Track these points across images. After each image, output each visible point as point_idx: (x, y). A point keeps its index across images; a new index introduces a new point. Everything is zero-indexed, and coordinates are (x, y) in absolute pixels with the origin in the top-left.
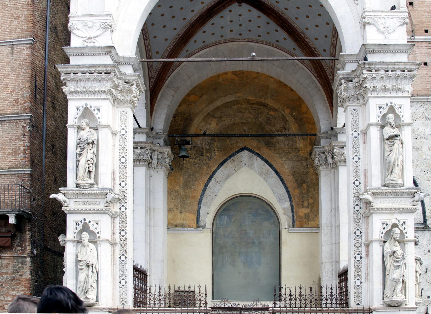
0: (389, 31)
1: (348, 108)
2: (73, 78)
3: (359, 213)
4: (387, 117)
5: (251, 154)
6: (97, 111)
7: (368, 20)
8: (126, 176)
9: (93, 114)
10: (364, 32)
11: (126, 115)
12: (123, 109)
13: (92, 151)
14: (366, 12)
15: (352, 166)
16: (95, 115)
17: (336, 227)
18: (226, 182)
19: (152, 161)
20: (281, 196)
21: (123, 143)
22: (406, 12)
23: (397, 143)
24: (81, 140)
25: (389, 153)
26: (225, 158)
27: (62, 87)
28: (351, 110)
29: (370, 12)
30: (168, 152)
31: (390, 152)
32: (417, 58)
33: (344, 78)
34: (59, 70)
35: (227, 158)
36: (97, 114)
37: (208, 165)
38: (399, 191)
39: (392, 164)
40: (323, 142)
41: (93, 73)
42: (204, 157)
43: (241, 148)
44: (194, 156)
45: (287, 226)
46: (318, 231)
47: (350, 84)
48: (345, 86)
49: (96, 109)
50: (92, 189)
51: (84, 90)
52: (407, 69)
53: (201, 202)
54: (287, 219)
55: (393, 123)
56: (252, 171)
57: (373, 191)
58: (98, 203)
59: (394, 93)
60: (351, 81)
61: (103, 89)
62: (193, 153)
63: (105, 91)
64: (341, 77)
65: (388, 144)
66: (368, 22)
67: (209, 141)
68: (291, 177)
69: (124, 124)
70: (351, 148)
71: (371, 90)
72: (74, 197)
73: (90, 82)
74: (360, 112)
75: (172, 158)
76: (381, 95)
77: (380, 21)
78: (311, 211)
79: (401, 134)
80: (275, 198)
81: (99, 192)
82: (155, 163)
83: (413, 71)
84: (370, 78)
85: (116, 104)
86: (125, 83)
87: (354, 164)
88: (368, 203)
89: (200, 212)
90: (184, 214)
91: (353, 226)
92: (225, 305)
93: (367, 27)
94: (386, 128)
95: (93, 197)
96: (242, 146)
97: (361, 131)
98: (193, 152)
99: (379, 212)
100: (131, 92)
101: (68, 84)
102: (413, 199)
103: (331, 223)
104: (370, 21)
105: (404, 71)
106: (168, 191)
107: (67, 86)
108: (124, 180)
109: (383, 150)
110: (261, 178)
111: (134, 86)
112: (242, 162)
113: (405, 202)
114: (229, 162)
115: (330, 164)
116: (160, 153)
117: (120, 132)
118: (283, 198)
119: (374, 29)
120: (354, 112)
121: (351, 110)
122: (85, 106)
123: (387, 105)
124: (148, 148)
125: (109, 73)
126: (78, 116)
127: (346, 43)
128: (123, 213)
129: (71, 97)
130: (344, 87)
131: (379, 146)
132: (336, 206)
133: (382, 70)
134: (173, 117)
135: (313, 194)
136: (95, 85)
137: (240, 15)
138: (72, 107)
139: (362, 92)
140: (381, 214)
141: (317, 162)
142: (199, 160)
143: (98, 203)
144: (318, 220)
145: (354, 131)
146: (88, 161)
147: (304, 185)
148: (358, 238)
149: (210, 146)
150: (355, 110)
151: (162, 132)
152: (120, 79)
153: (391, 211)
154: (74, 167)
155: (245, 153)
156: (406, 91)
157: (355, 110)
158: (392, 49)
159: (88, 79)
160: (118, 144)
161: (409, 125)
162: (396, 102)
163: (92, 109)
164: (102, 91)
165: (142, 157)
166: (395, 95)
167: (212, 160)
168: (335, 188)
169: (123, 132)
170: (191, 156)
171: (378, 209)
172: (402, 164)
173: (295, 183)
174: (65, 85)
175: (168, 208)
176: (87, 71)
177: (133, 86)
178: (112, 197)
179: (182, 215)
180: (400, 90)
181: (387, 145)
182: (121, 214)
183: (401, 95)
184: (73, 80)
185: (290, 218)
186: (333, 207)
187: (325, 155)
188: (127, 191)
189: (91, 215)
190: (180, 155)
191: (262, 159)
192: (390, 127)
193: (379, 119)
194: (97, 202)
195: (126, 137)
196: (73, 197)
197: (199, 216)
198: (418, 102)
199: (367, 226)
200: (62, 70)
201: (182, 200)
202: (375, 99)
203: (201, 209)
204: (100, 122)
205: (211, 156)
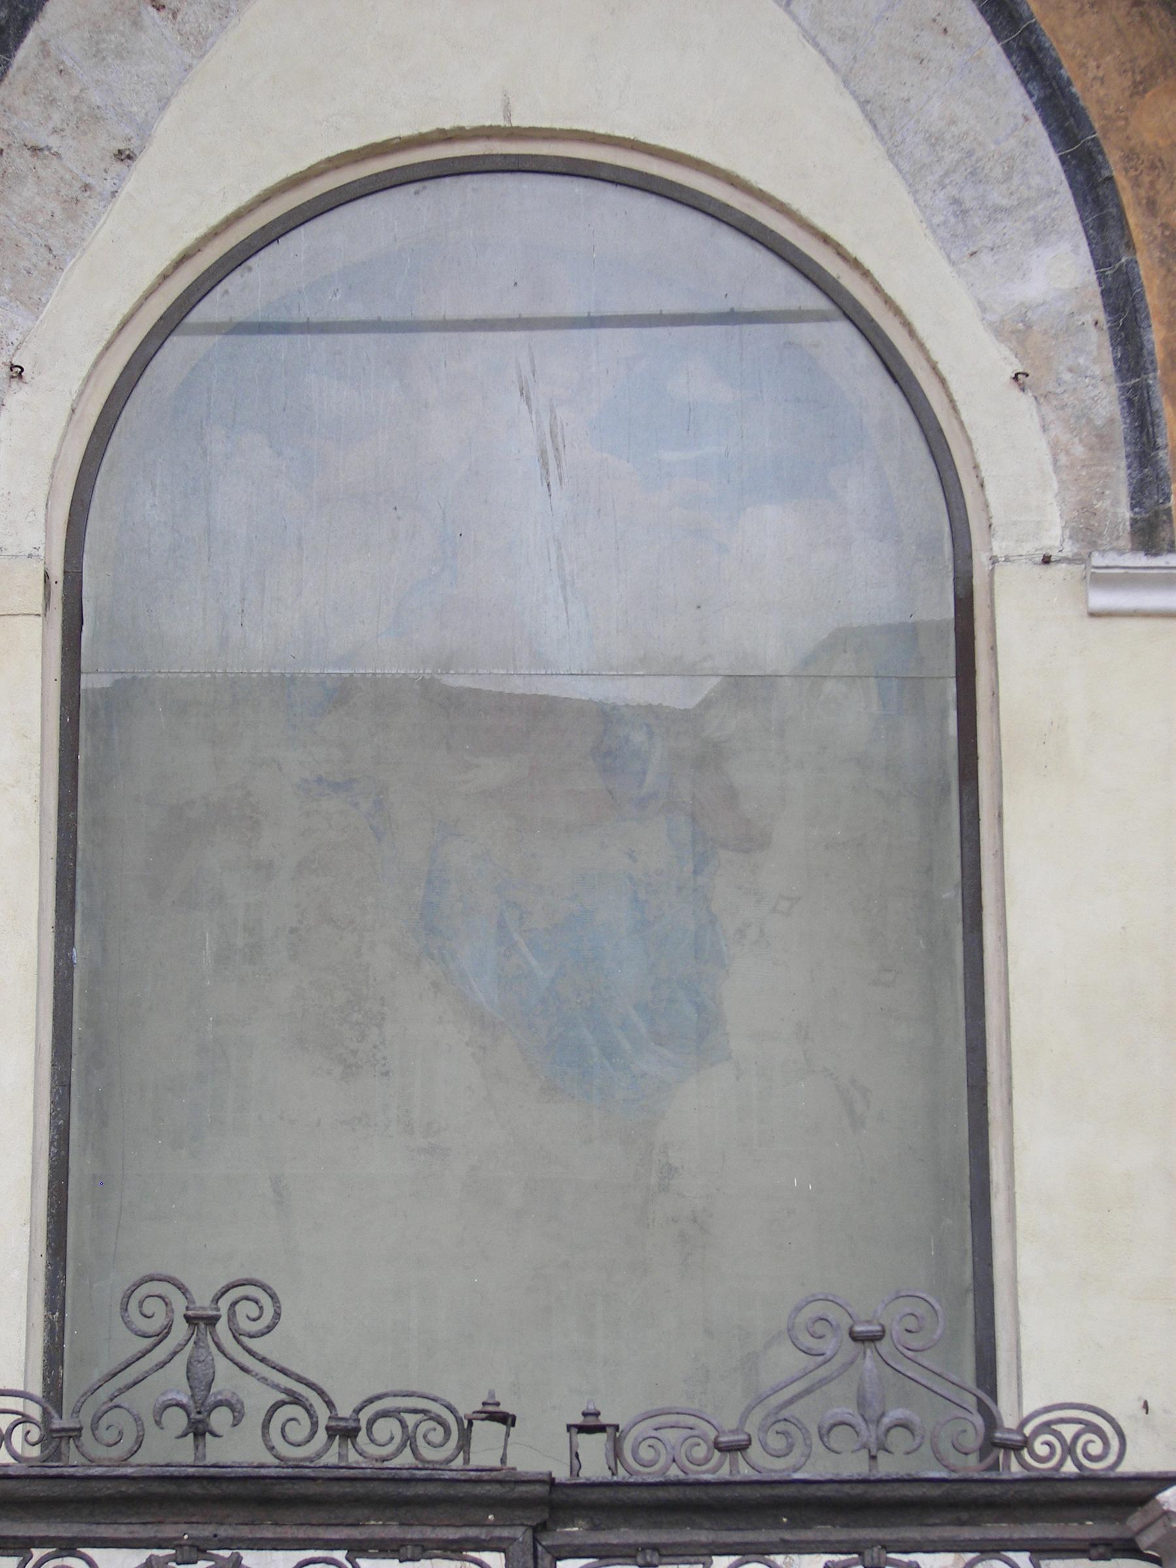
20: (975, 175)
92: (199, 1430)
118: (997, 197)
185: (1102, 440)
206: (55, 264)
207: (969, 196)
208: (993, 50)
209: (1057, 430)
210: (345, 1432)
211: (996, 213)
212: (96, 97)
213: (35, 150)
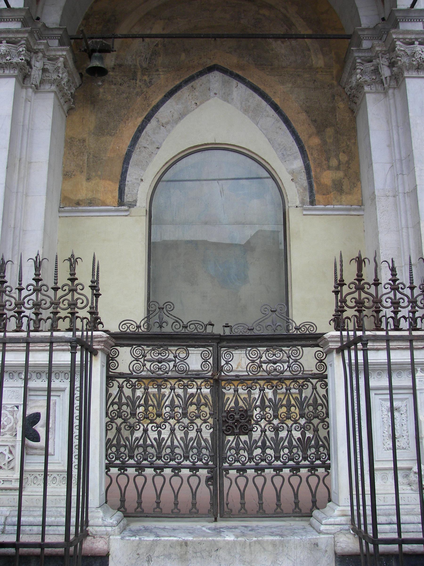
17: (404, 197)
26: (178, 82)
30: (65, 58)
35: (181, 83)
37: (145, 95)
43: (208, 66)
44: (119, 80)
45: (298, 203)
53: (130, 159)
56: (229, 105)
62: (117, 76)
67: (148, 56)
68: (303, 116)
78: (346, 175)
90: (94, 182)
96: (210, 63)
98: (117, 73)
110: (246, 117)
114: (185, 91)
124: (23, 42)
134: (84, 19)
135: (348, 146)
142: (129, 87)
144: (359, 191)
147: (328, 130)
149: (149, 63)
165: (8, 58)
167: (153, 86)
170: (113, 80)
173: (312, 126)
179: (90, 183)
185: (305, 189)
191: (247, 86)
201: (91, 156)
203: (128, 173)
205: (152, 79)
206: (147, 164)
207: (284, 153)
208: (288, 132)
209: (298, 188)
210: (185, 327)
211: (288, 155)
212: (154, 140)
213: (145, 147)
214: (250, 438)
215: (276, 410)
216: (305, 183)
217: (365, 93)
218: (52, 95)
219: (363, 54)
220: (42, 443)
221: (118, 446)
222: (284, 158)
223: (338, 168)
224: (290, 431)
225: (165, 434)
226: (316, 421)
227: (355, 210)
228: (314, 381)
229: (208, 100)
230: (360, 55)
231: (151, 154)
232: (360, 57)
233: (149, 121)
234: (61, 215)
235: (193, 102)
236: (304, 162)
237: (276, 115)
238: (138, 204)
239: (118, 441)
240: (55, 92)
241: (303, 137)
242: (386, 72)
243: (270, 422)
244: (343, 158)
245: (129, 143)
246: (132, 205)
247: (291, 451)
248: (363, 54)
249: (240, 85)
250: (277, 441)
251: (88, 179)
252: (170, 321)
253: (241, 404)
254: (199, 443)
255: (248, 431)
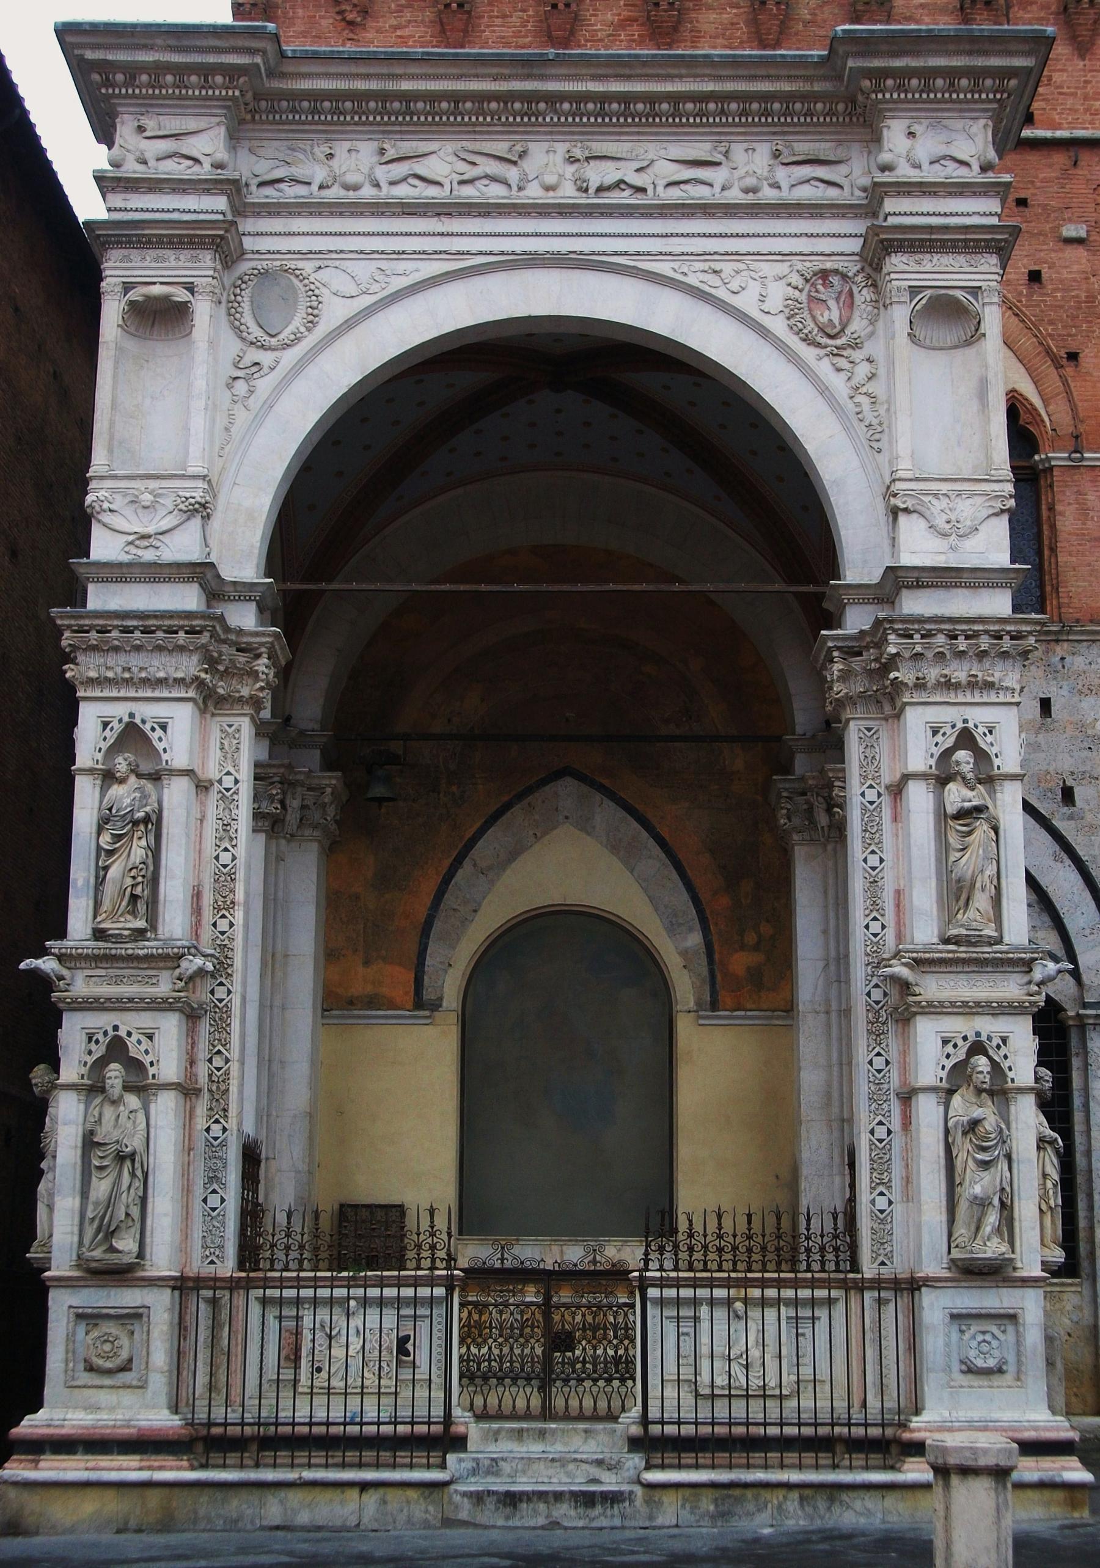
0: (961, 532)
1: (852, 724)
2: (95, 643)
3: (881, 1008)
4: (954, 758)
5: (585, 788)
6: (159, 732)
7: (904, 503)
8: (233, 903)
9: (147, 740)
10: (894, 528)
11: (237, 736)
12: (231, 720)
13: (143, 843)
14: (899, 480)
15: (862, 880)
16: (155, 743)
18: (508, 872)
19: (285, 816)
21: (227, 811)
22: (1008, 481)
23: (982, 829)
24: (114, 811)
25: (958, 855)
27: (66, 667)
28: (860, 730)
29: (911, 480)
31: (961, 853)
32: (1091, 513)
33: (838, 648)
34: (59, 622)
36: (160, 739)
38: (987, 956)
39: (967, 884)
40: (801, 764)
41: (153, 632)
42: (441, 795)
46: (789, 1022)
47: (856, 663)
48: (841, 667)
49: (156, 726)
50: (141, 944)
51: (127, 675)
52: (1008, 632)
54: (693, 983)
55: (970, 775)
57: (915, 955)
58: (154, 981)
59: (972, 693)
60: (860, 654)
61: (180, 675)
63: (183, 679)
64: (830, 644)
65: (958, 831)
66: (903, 506)
69: (229, 761)
70: (860, 831)
71: (911, 684)
72: (88, 965)
73: (142, 655)
74: (884, 734)
75: (344, 799)
76: (938, 698)
77: (937, 506)
79: (994, 801)
80: (658, 921)
81: (160, 951)
82: (294, 821)
83: (1025, 636)
84: (907, 654)
85: (212, 708)
86: (238, 650)
87: (867, 875)
88: (905, 986)
89: (425, 959)
91: (865, 1045)
93: (902, 519)
94: (952, 786)
95: (141, 966)
97: (887, 787)
99: (932, 1010)
100: (254, 675)
101: (81, 658)
102: (1026, 979)
103: (828, 1001)
104: (909, 504)
105: (1000, 638)
106: (328, 897)
107: (77, 664)
108: (227, 914)
109: (943, 846)
111: (264, 660)
112: (557, 810)
113: (1006, 984)
115: (823, 828)
116: (309, 789)
117: (220, 781)
119: (922, 524)
120: (869, 734)
121: (860, 730)
122: (126, 719)
123: (953, 726)
125: (199, 632)
126: (104, 746)
127: (845, 550)
128: (220, 1005)
129: (88, 694)
130: (839, 671)
131: (932, 834)
132: (842, 950)
133: (939, 636)
136: (156, 663)
137: (558, 411)
138: (89, 717)
139: (887, 687)
140: (939, 1017)
141: (782, 821)
143: (154, 981)
145: (867, 785)
146: (131, 869)
148: (879, 1076)
150: (869, 730)
151: (317, 726)
152: (224, 642)
153: (968, 1010)
154: (88, 881)
155: (567, 790)
156: (1007, 688)
157: (869, 730)
158: (966, 578)
159: (138, 649)
160: (212, 812)
161: (1013, 777)
162: (978, 717)
163: (147, 728)
164: (175, 679)
166: (977, 699)
168: (837, 898)
169: (228, 782)
171: (930, 1004)
172: (995, 882)
174: (73, 661)
175: (326, 947)
176: (136, 628)
177: (260, 661)
178: (195, 968)
180: (989, 686)
181: (954, 833)
182: (216, 1006)
183: (993, 698)
184: (94, 648)
186: (833, 954)
187: (807, 802)
188: (235, 943)
189: (133, 1014)
190: (370, 795)
192: (962, 784)
193: (933, 762)
194: (150, 977)
195: (235, 797)
196: (83, 965)
197: (424, 972)
198: (1094, 641)
199: (904, 1044)
200: (66, 622)
202: (920, 709)
204: (167, 762)
207: (674, 921)
208: (681, 884)
209: (694, 979)
210: (522, 1263)
211: (680, 925)
214: (574, 1354)
215: (594, 1333)
216: (705, 971)
217: (793, 845)
218: (315, 846)
219: (792, 785)
220: (412, 1357)
221: (468, 1360)
222: (672, 928)
223: (756, 948)
224: (605, 1349)
225: (506, 1350)
226: (626, 1342)
227: (778, 1018)
228: (626, 1309)
229: (554, 828)
230: (787, 786)
231: (465, 922)
232: (786, 789)
233: (461, 863)
234: (325, 1021)
235: (531, 833)
236: (705, 937)
237: (663, 856)
238: (445, 1004)
239: (468, 1356)
240: (319, 842)
241: (704, 896)
242: (823, 820)
243: (589, 1342)
244: (766, 929)
245: (429, 904)
246: (435, 1006)
247: (605, 1366)
248: (792, 785)
249: (608, 803)
250: (595, 1358)
251: (367, 963)
252: (510, 1259)
253: (567, 1327)
254: (532, 1359)
255: (573, 1350)
